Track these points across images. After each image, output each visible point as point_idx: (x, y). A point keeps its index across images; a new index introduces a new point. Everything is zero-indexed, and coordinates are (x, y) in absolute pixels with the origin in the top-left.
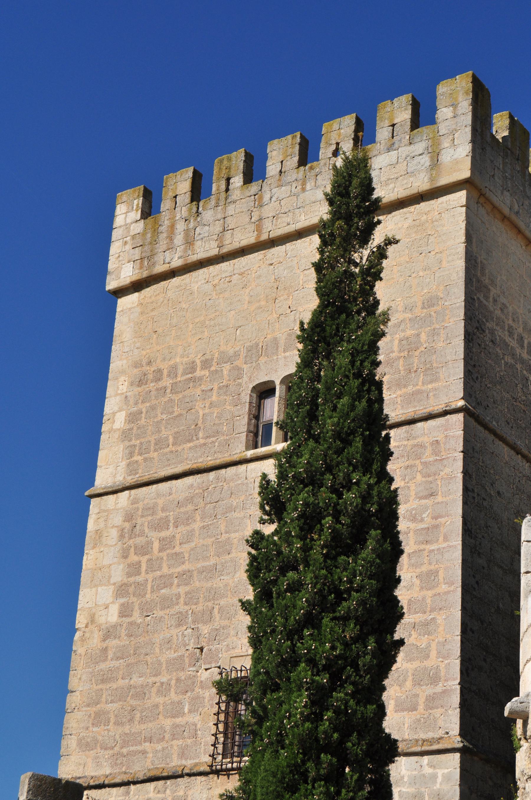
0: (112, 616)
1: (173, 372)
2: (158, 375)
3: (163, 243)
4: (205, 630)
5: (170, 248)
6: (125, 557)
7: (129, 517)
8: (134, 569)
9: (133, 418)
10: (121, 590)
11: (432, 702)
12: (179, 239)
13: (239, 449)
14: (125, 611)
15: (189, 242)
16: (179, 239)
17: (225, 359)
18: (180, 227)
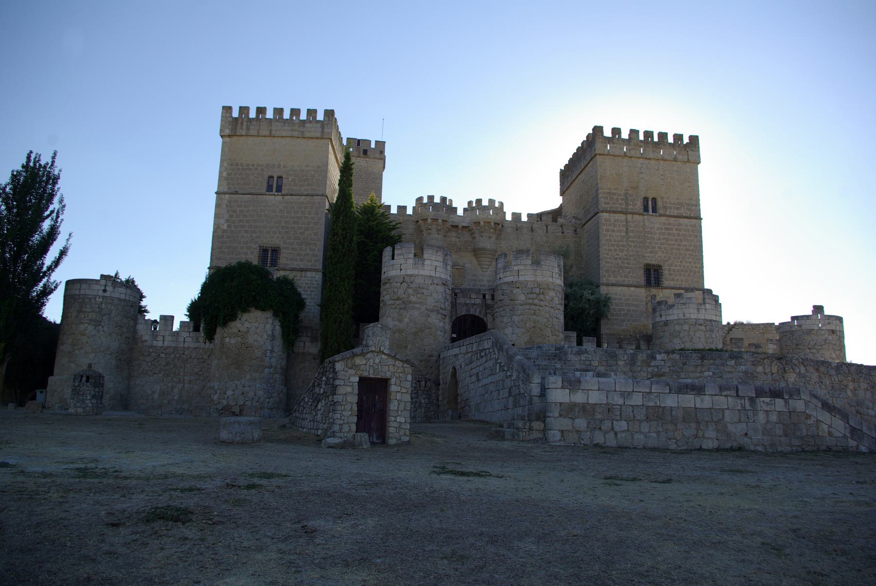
0: (225, 227)
1: (242, 165)
2: (237, 164)
3: (239, 126)
4: (254, 235)
5: (242, 129)
6: (228, 212)
7: (229, 202)
8: (231, 216)
9: (229, 174)
10: (227, 221)
11: (316, 261)
12: (244, 127)
13: (264, 191)
14: (229, 226)
15: (248, 129)
16: (244, 127)
17: (258, 165)
18: (245, 123)
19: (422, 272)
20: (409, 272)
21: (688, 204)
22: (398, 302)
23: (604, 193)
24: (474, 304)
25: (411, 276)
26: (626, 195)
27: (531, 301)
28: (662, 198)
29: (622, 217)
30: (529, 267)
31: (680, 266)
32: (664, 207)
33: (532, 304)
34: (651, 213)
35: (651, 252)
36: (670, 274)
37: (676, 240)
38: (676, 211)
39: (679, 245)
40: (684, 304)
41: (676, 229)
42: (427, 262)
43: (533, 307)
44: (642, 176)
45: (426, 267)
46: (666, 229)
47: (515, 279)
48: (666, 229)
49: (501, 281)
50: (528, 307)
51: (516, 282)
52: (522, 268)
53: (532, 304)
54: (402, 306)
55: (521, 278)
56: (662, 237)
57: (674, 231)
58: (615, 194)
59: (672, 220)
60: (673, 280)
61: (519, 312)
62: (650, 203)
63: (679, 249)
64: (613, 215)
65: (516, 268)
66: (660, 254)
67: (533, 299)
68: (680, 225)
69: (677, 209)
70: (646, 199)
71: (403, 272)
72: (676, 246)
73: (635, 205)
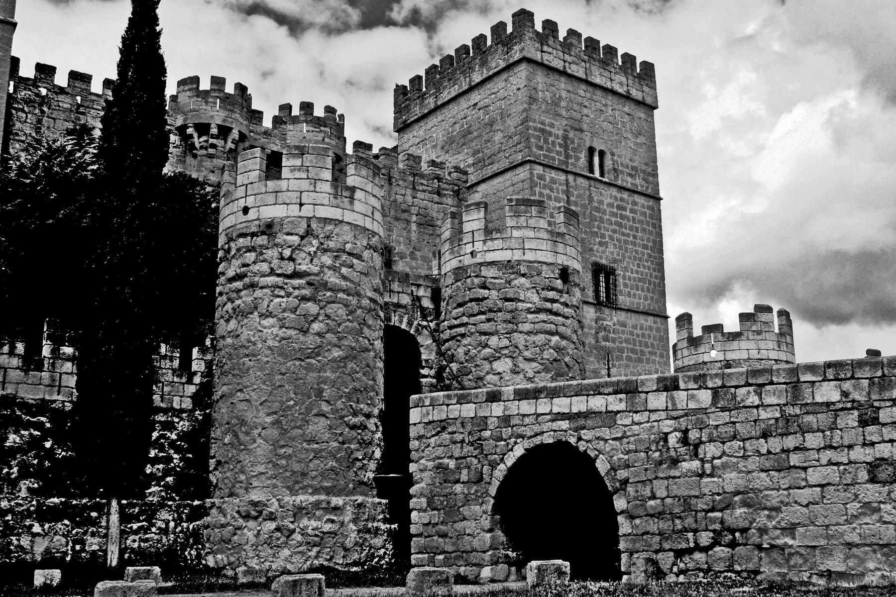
19: (349, 217)
20: (322, 212)
21: (644, 172)
22: (296, 282)
23: (535, 129)
24: (398, 306)
25: (326, 221)
26: (565, 138)
27: (548, 305)
28: (613, 154)
29: (562, 177)
30: (545, 235)
31: (637, 272)
32: (615, 170)
33: (550, 312)
34: (597, 174)
35: (600, 244)
36: (625, 285)
37: (631, 228)
38: (629, 179)
39: (635, 237)
40: (759, 333)
41: (632, 211)
42: (359, 195)
43: (552, 318)
44: (585, 111)
45: (358, 206)
46: (619, 207)
47: (517, 256)
48: (619, 207)
49: (479, 259)
50: (542, 316)
51: (519, 262)
52: (531, 234)
53: (550, 312)
54: (306, 292)
55: (530, 256)
56: (613, 219)
57: (628, 213)
58: (550, 134)
59: (625, 195)
60: (629, 295)
61: (527, 327)
62: (596, 160)
63: (634, 244)
64: (548, 170)
65: (516, 233)
66: (611, 248)
67: (553, 301)
68: (635, 203)
69: (631, 176)
70: (591, 150)
71: (307, 211)
72: (631, 239)
73: (577, 158)
